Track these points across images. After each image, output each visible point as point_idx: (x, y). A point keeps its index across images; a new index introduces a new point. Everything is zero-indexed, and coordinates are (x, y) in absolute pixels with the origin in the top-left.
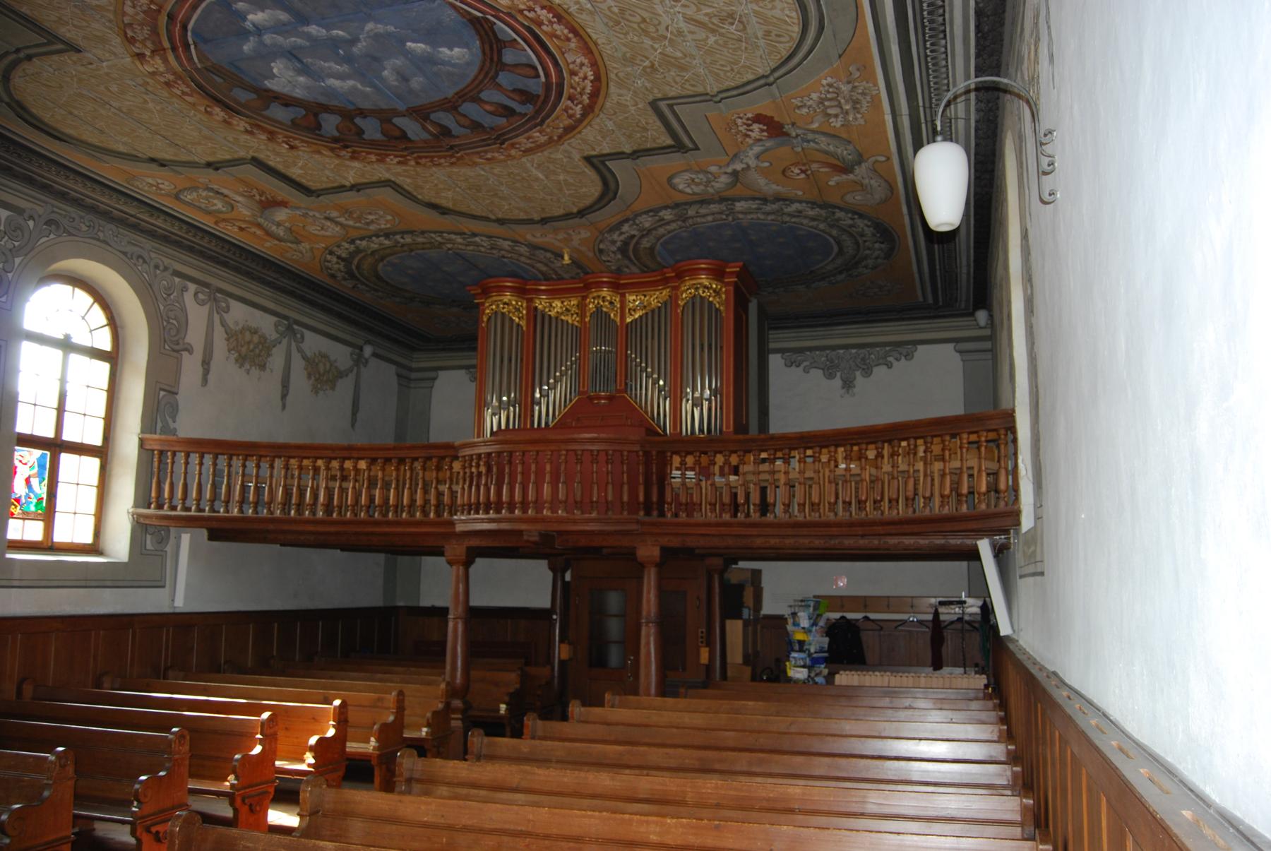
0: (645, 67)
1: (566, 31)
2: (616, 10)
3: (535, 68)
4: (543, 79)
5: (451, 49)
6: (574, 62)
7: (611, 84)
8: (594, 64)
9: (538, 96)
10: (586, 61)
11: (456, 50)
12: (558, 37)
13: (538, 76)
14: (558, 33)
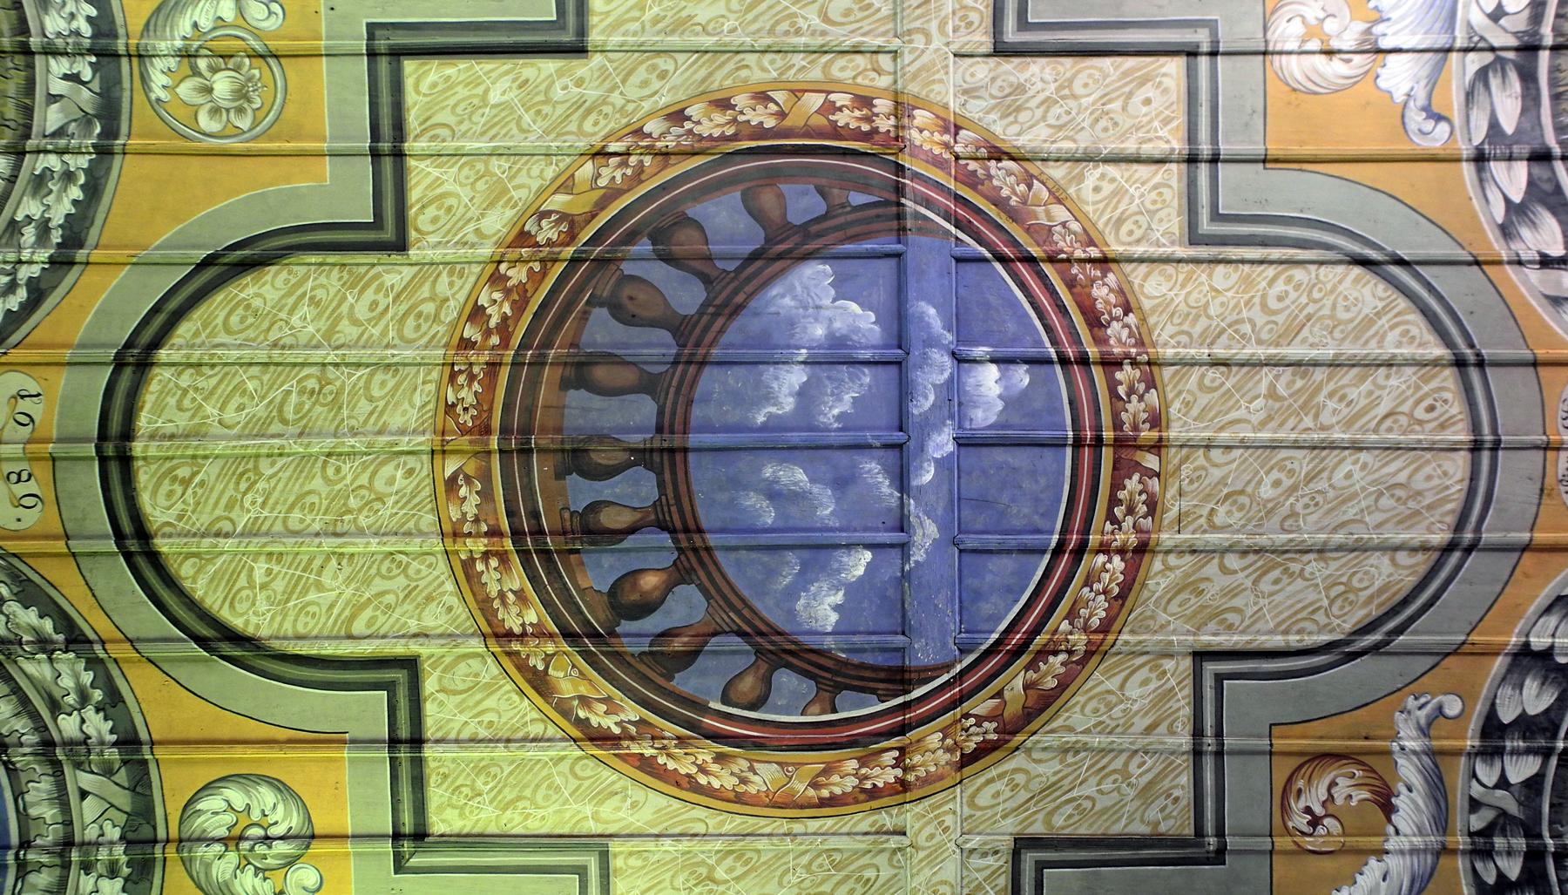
0: (712, 869)
1: (838, 791)
2: (870, 874)
3: (753, 707)
4: (715, 705)
5: (836, 608)
6: (752, 770)
7: (676, 804)
8: (739, 799)
9: (671, 678)
10: (752, 789)
11: (834, 617)
12: (826, 772)
13: (725, 700)
14: (835, 778)
